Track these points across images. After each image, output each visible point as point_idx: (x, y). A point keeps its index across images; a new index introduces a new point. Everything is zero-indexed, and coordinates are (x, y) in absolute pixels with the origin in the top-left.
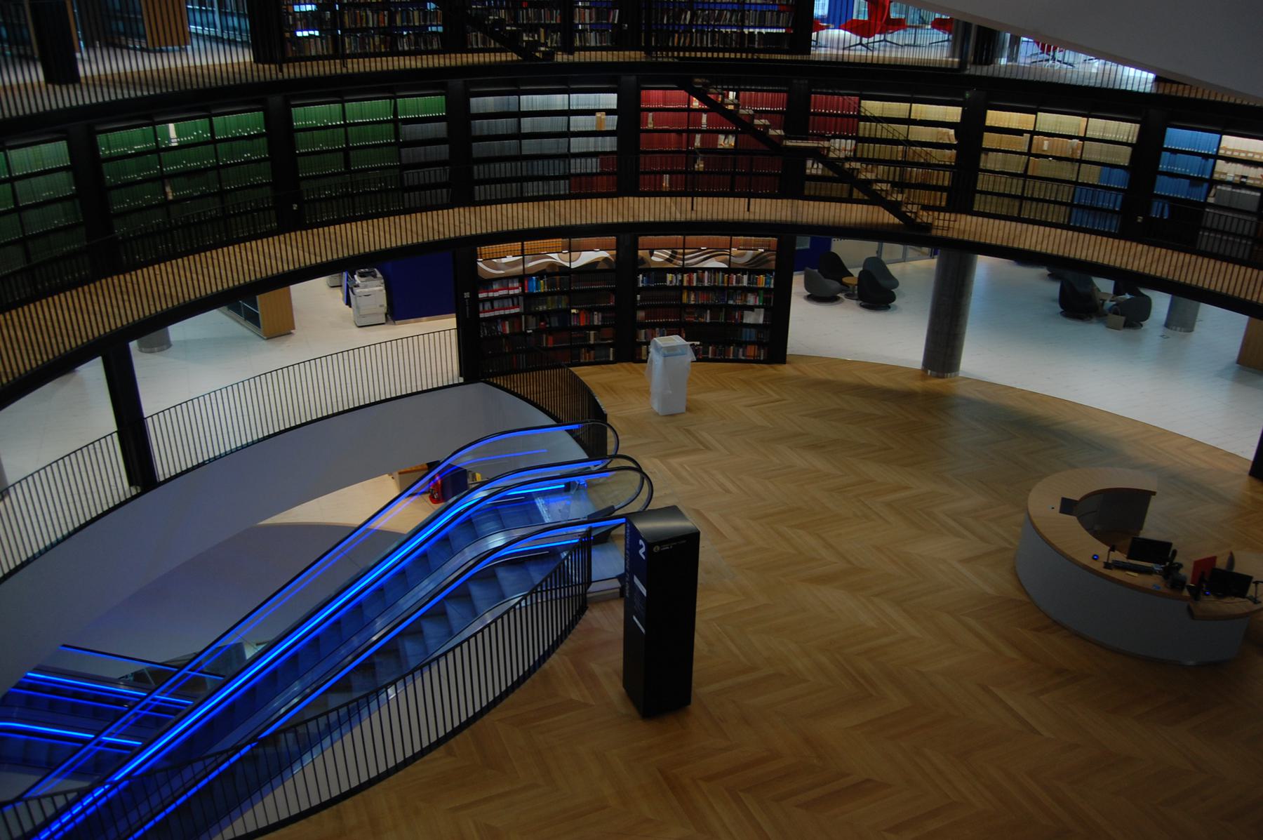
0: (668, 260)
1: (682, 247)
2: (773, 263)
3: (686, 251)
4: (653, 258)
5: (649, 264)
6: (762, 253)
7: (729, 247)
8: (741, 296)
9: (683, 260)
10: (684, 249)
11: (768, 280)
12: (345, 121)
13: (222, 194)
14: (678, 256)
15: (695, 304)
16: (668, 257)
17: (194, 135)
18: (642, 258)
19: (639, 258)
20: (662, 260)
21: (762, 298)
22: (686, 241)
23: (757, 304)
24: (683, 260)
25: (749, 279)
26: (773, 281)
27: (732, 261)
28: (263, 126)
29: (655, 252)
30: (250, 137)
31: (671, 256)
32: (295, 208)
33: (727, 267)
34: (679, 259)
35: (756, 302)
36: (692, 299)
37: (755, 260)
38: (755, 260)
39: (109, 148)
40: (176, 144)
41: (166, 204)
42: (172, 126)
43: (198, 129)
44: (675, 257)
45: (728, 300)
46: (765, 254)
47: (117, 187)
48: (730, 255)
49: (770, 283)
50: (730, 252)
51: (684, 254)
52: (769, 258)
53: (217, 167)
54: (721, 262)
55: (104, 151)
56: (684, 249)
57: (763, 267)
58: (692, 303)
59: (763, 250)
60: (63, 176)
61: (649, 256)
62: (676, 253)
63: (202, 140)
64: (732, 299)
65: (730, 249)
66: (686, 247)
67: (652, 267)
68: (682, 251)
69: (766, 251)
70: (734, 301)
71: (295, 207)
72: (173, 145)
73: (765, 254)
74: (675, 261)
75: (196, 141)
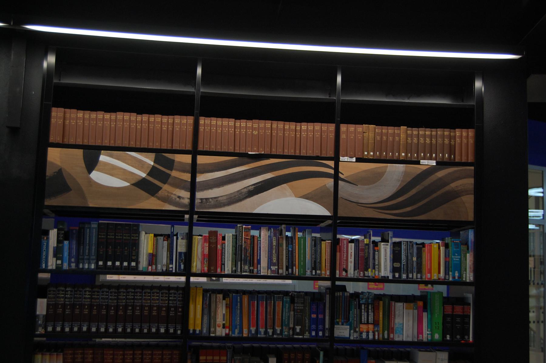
0: (142, 184)
1: (189, 147)
2: (469, 200)
3: (201, 160)
4: (96, 176)
5: (81, 194)
6: (431, 171)
7: (331, 154)
8: (375, 310)
9: (193, 187)
10: (195, 152)
11: (456, 258)
14: (174, 173)
15: (227, 338)
16: (144, 175)
18: (60, 172)
19: (49, 172)
20: (126, 184)
21: (438, 318)
22: (201, 129)
23: (426, 336)
24: (193, 187)
25: (396, 256)
26: (469, 258)
27: (341, 194)
29: (104, 158)
31: (153, 172)
33: (326, 213)
34: (179, 184)
35: (420, 331)
36: (220, 320)
37: (400, 199)
38: (400, 199)
44: (165, 178)
45: (333, 324)
46: (441, 174)
48: (336, 177)
49: (460, 267)
50: (336, 168)
51: (194, 169)
52: (453, 185)
54: (307, 197)
56: (195, 152)
57: (437, 214)
58: (221, 332)
59: (434, 163)
61: (85, 170)
62: (170, 165)
64: (347, 321)
65: (336, 160)
66: (200, 148)
67: (92, 204)
68: (187, 159)
69: (441, 164)
70: (353, 328)
73: (441, 174)
74: (166, 188)
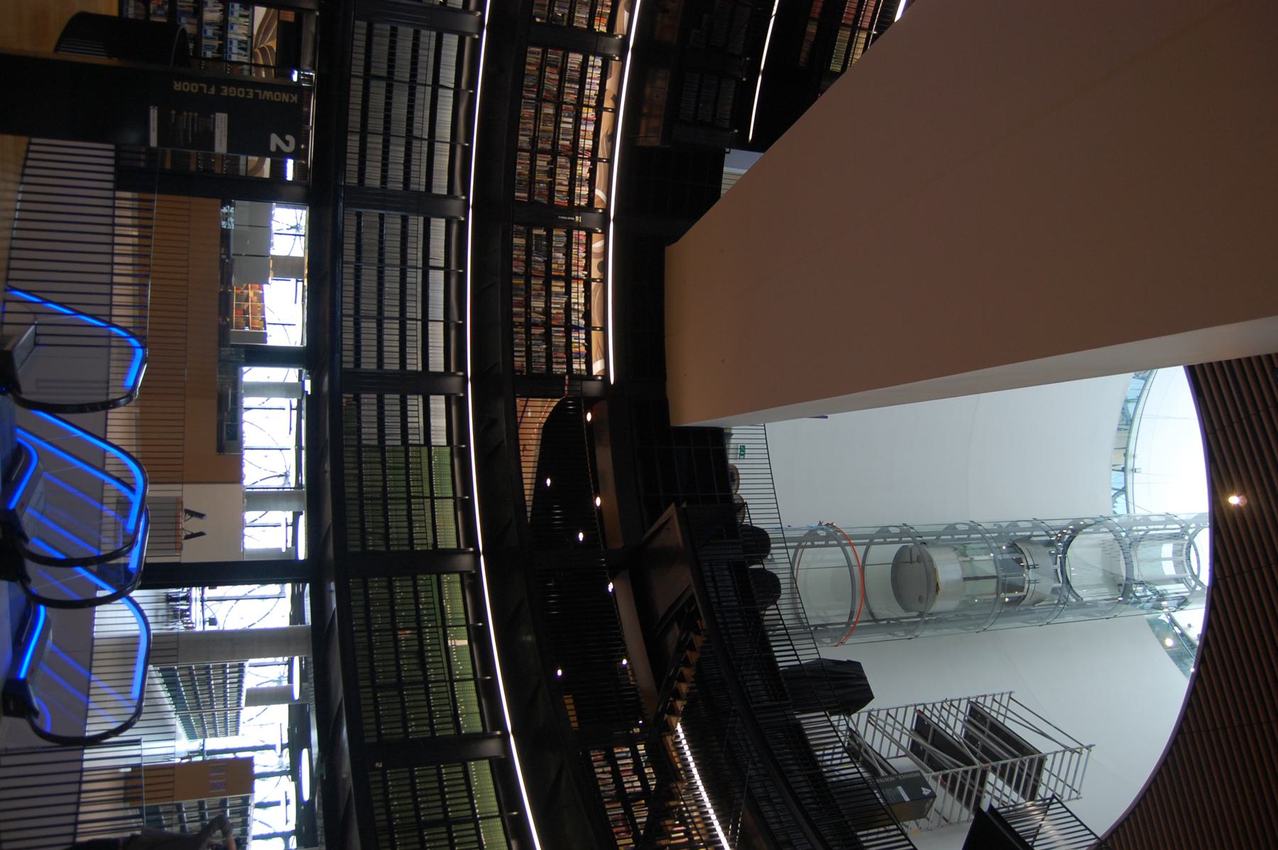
12: (480, 819)
13: (399, 686)
17: (457, 662)
28: (469, 730)
30: (456, 716)
32: (377, 764)
39: (449, 582)
40: (450, 644)
41: (395, 630)
42: (465, 642)
43: (463, 666)
47: (415, 586)
53: (426, 681)
55: (445, 578)
60: (430, 541)
63: (453, 668)
71: (379, 765)
72: (449, 641)
75: (452, 663)
